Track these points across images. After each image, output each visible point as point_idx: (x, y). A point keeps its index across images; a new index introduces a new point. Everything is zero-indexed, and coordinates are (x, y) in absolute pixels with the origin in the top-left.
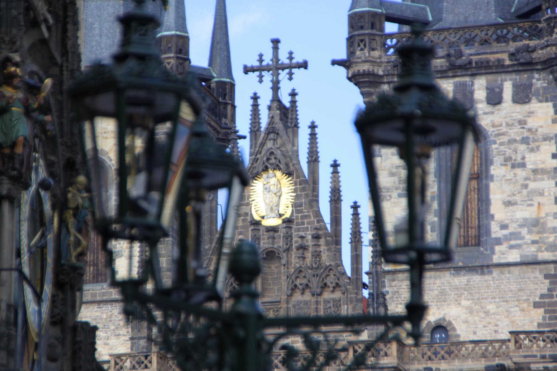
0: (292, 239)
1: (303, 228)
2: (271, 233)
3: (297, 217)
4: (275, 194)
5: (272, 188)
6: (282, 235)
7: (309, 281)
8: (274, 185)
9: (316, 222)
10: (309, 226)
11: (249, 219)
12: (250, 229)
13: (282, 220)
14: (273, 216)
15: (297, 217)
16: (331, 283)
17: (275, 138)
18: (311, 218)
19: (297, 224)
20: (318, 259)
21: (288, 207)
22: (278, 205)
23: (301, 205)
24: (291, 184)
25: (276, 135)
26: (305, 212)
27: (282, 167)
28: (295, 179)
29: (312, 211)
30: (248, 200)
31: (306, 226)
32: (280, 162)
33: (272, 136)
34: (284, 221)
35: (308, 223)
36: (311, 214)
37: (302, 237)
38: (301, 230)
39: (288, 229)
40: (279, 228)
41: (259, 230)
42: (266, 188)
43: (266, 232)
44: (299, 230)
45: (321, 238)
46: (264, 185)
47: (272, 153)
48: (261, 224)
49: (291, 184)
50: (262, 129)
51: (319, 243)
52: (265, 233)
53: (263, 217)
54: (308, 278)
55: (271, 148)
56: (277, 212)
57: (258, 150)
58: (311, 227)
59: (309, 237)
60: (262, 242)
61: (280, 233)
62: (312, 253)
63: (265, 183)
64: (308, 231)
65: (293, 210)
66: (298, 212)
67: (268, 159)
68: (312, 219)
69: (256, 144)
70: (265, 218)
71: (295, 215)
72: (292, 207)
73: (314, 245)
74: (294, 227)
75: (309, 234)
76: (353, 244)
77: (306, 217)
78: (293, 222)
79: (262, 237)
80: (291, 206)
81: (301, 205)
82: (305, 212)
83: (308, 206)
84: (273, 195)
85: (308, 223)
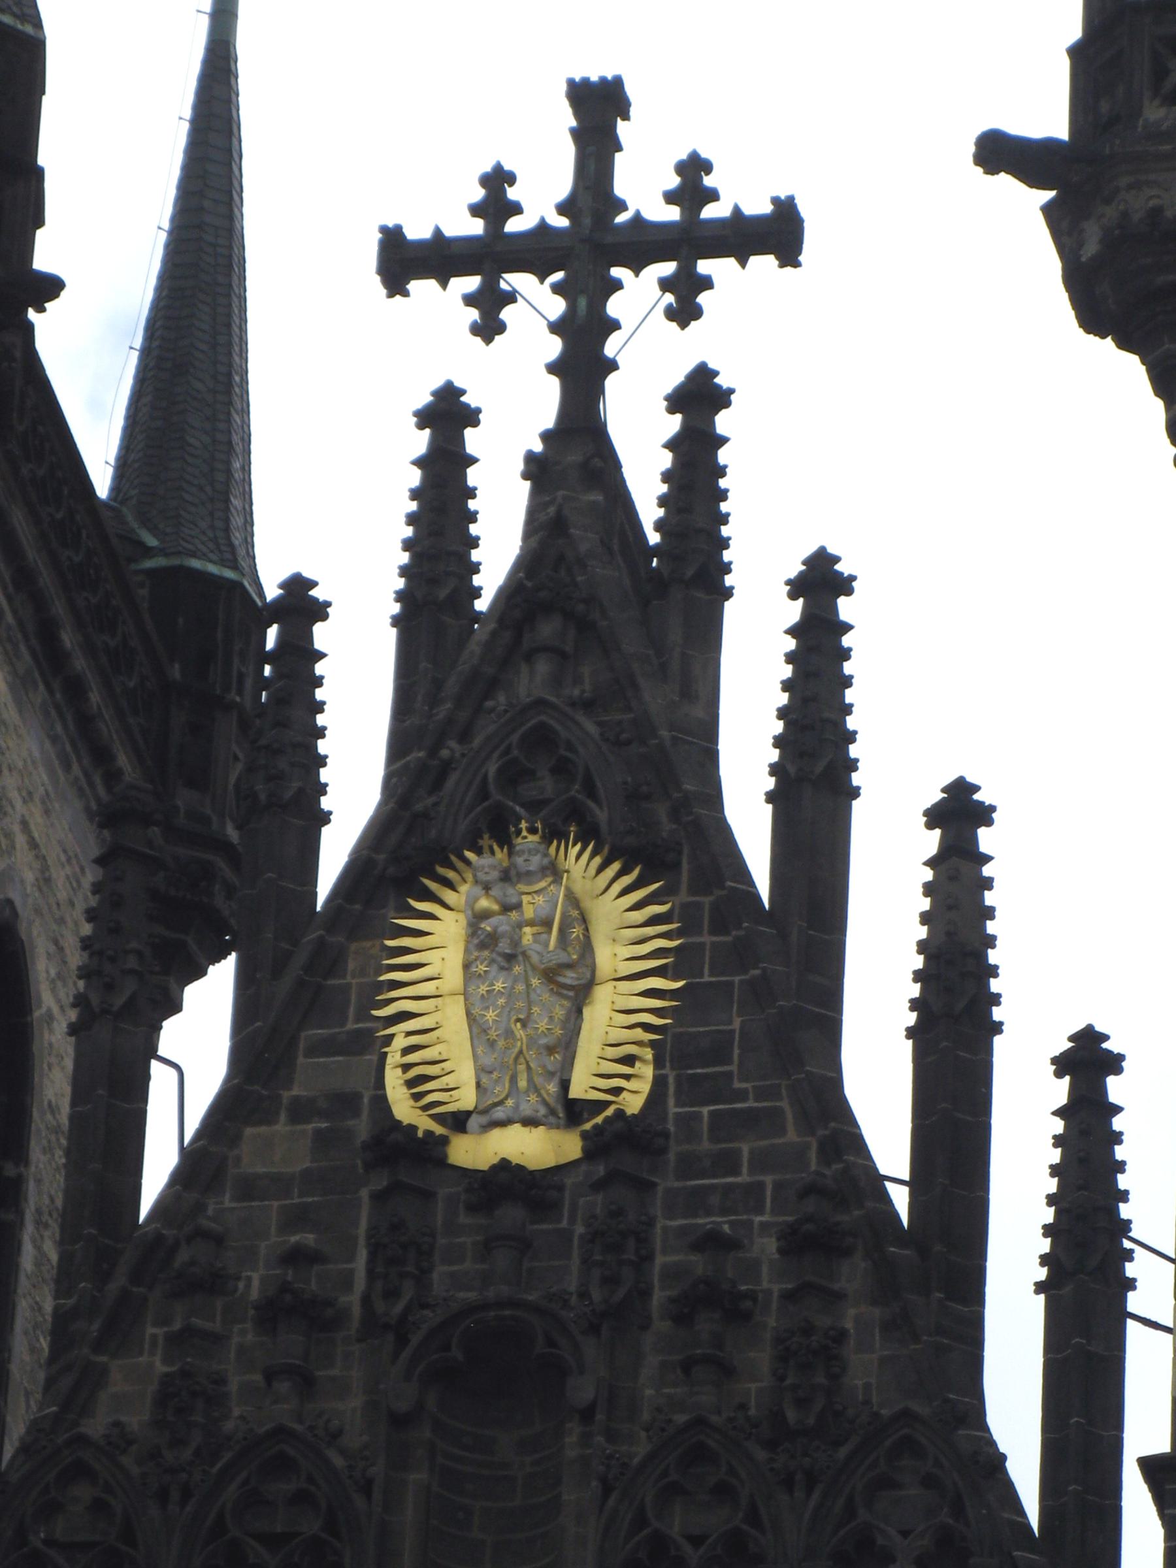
0: (650, 1257)
2: (511, 1215)
3: (688, 1122)
4: (550, 975)
6: (580, 1229)
7: (753, 1517)
8: (547, 924)
9: (813, 1155)
10: (769, 1180)
11: (362, 1127)
12: (364, 1193)
13: (585, 1136)
14: (526, 1110)
15: (688, 1122)
16: (905, 1534)
17: (569, 648)
18: (783, 1131)
19: (688, 1166)
20: (820, 1379)
21: (629, 1060)
22: (567, 1046)
23: (718, 1051)
24: (653, 921)
26: (742, 1095)
27: (602, 815)
28: (684, 897)
30: (363, 1014)
31: (744, 1178)
33: (547, 629)
34: (595, 1147)
35: (761, 1162)
36: (785, 1104)
37: (712, 1242)
38: (715, 1200)
40: (561, 1188)
41: (428, 1195)
43: (472, 1209)
44: (696, 1202)
45: (847, 1252)
46: (485, 915)
47: (542, 739)
48: (441, 1162)
49: (653, 921)
50: (482, 605)
51: (836, 1286)
52: (463, 1219)
53: (459, 1122)
55: (540, 703)
56: (553, 1088)
58: (778, 1186)
59: (767, 1247)
60: (440, 1273)
61: (564, 1224)
63: (484, 903)
64: (760, 1210)
65: (659, 1083)
66: (692, 1090)
67: (513, 775)
68: (792, 1135)
69: (438, 684)
70: (473, 1123)
71: (673, 1109)
72: (658, 1062)
73: (788, 1297)
74: (667, 1182)
75: (764, 1226)
76: (1068, 1289)
77: (750, 1120)
78: (663, 1151)
79: (442, 1241)
80: (648, 1054)
81: (718, 1051)
82: (742, 1095)
84: (535, 982)
85: (761, 1162)
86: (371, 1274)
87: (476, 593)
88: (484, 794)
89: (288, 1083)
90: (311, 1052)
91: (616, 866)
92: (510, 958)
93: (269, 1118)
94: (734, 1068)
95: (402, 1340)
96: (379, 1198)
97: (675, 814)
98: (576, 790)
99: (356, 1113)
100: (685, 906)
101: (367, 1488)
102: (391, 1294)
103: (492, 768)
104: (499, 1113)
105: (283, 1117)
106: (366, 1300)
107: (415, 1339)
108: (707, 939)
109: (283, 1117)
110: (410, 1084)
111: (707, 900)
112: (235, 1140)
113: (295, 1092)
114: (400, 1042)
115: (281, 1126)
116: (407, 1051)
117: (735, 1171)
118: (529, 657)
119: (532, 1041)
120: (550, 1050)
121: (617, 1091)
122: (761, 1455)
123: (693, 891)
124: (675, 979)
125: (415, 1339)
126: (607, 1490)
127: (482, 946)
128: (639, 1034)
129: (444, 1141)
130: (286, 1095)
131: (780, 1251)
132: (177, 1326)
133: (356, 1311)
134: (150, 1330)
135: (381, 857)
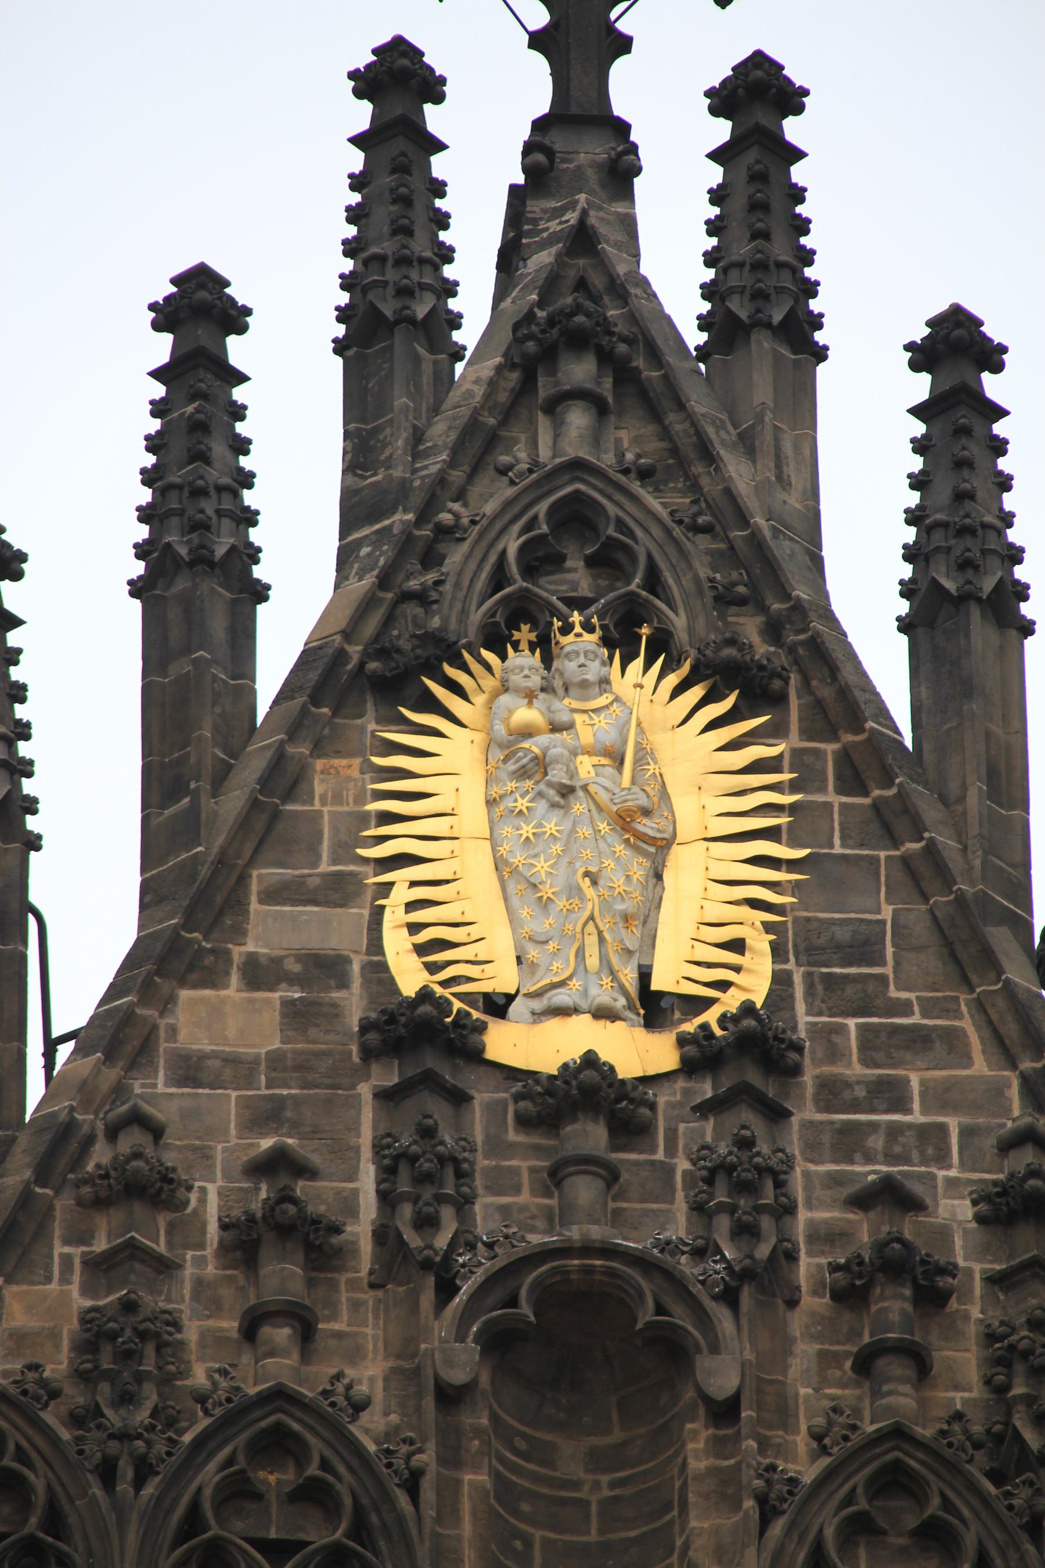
0: (790, 1210)
1: (894, 1131)
5: (585, 766)
12: (365, 1090)
13: (682, 1041)
18: (967, 1060)
21: (737, 946)
24: (755, 767)
25: (608, 383)
26: (905, 1008)
29: (980, 1006)
30: (344, 850)
31: (917, 1117)
32: (653, 582)
36: (967, 1024)
38: (877, 1142)
39: (747, 1117)
41: (459, 1098)
42: (540, 764)
43: (524, 1122)
46: (527, 732)
48: (476, 1056)
49: (755, 767)
54: (970, 1539)
55: (577, 467)
56: (629, 977)
57: (441, 480)
62: (991, 1337)
64: (942, 1159)
65: (781, 981)
68: (980, 1066)
70: (516, 1008)
72: (778, 951)
75: (951, 1182)
78: (796, 1070)
79: (482, 1162)
82: (905, 1008)
83: (931, 961)
84: (603, 826)
86: (386, 1198)
87: (455, 321)
88: (499, 579)
89: (239, 933)
90: (273, 895)
91: (696, 693)
92: (567, 791)
93: (213, 979)
94: (888, 970)
95: (446, 1290)
96: (385, 1096)
97: (773, 631)
99: (344, 984)
100: (797, 754)
101: (412, 1485)
102: (426, 1223)
103: (512, 545)
104: (561, 998)
105: (235, 978)
106: (382, 1235)
107: (466, 1289)
108: (836, 800)
109: (235, 978)
110: (421, 950)
111: (830, 748)
112: (168, 1004)
113: (250, 947)
114: (401, 894)
115: (233, 991)
116: (412, 906)
117: (901, 1104)
118: (554, 406)
119: (605, 904)
120: (626, 918)
121: (723, 986)
123: (807, 733)
124: (793, 844)
125: (466, 1289)
126: (767, 1513)
127: (522, 774)
128: (746, 911)
129: (481, 1028)
130: (237, 953)
131: (980, 1219)
132: (101, 1245)
133: (366, 1247)
134: (59, 1249)
135: (355, 651)
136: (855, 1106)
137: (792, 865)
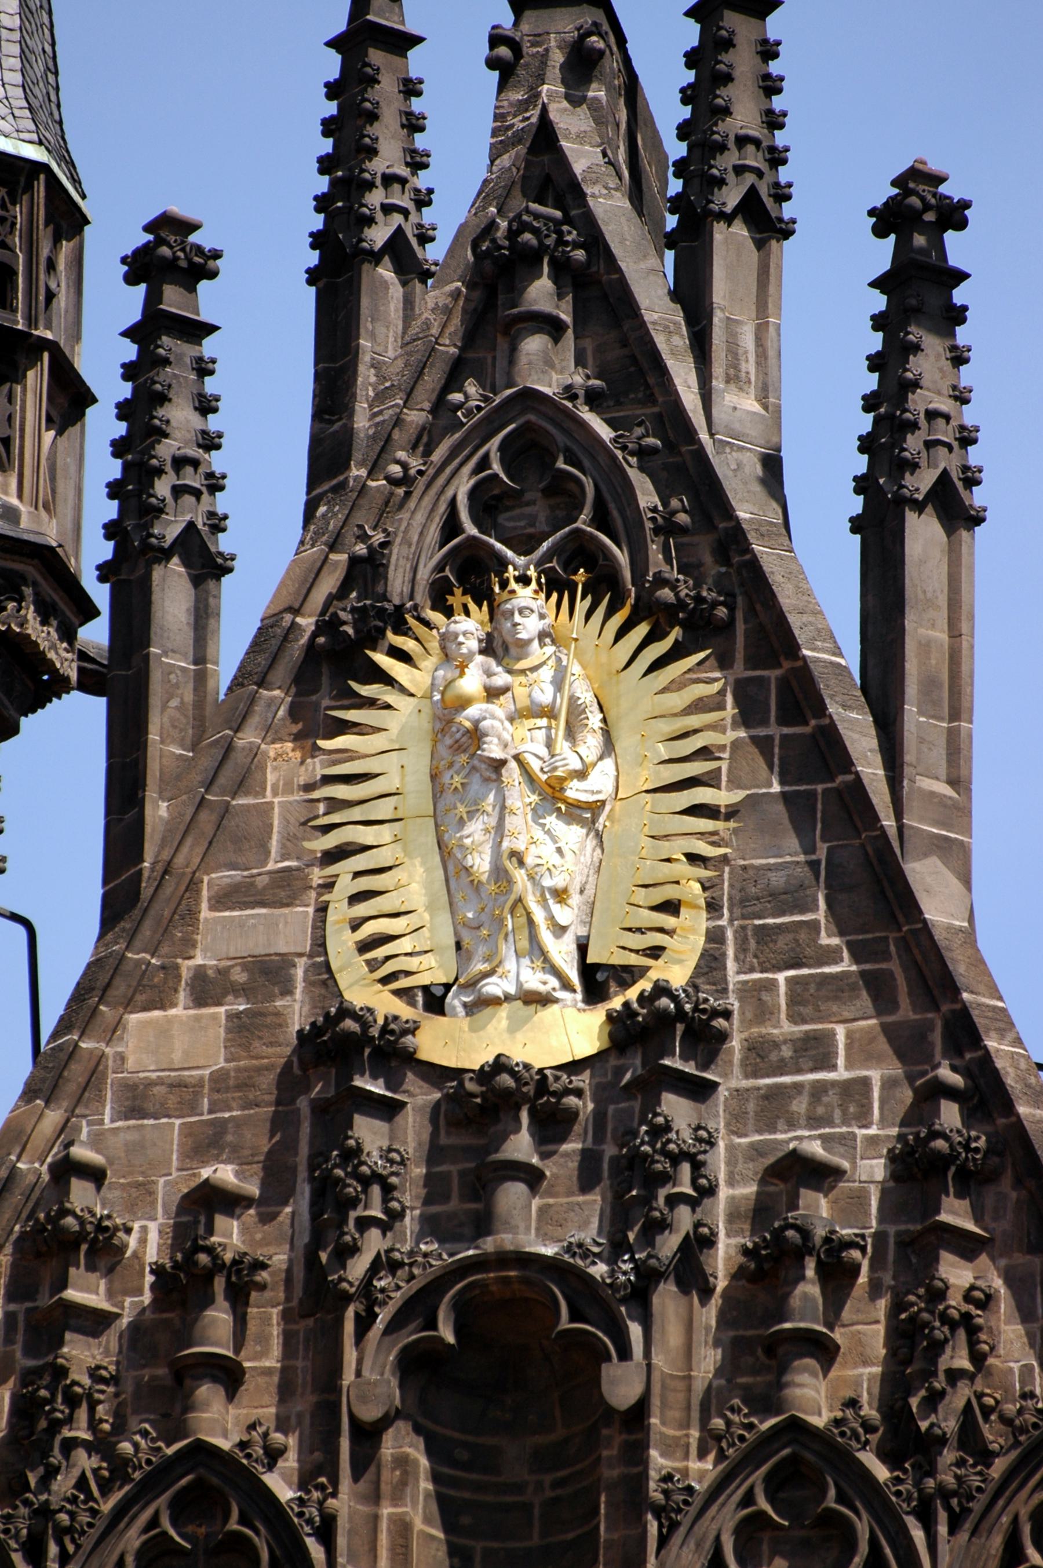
0: (711, 1191)
1: (819, 1090)
21: (671, 907)
31: (841, 1073)
36: (894, 966)
64: (863, 1118)
70: (455, 1001)
71: (733, 974)
75: (872, 1140)
78: (723, 1037)
88: (451, 527)
89: (187, 947)
91: (642, 630)
98: (583, 522)
103: (463, 486)
105: (182, 996)
109: (182, 996)
110: (364, 947)
111: (773, 674)
113: (199, 961)
114: (346, 886)
115: (180, 1011)
116: (356, 898)
117: (826, 1062)
122: (882, 1473)
123: (752, 662)
127: (458, 748)
130: (186, 967)
136: (781, 1069)
137: (732, 813)
